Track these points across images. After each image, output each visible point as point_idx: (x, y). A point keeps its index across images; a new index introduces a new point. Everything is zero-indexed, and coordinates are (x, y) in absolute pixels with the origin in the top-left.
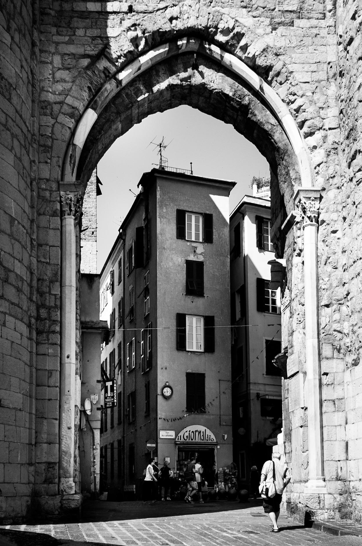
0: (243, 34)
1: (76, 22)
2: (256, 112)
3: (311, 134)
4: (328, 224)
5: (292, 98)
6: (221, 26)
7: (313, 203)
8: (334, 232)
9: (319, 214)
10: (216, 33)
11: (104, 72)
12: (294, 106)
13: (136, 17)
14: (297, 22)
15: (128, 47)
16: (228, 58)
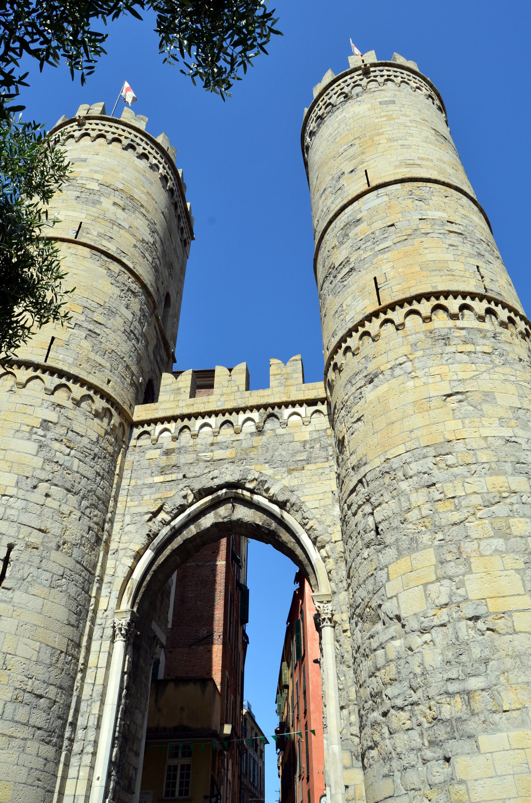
0: (266, 481)
1: (146, 491)
2: (281, 535)
3: (323, 547)
4: (340, 624)
5: (305, 521)
6: (250, 477)
7: (325, 606)
8: (345, 631)
9: (333, 615)
10: (245, 483)
11: (161, 522)
12: (307, 527)
13: (188, 481)
14: (307, 467)
15: (180, 501)
16: (256, 497)
